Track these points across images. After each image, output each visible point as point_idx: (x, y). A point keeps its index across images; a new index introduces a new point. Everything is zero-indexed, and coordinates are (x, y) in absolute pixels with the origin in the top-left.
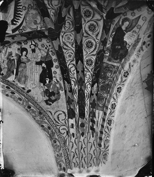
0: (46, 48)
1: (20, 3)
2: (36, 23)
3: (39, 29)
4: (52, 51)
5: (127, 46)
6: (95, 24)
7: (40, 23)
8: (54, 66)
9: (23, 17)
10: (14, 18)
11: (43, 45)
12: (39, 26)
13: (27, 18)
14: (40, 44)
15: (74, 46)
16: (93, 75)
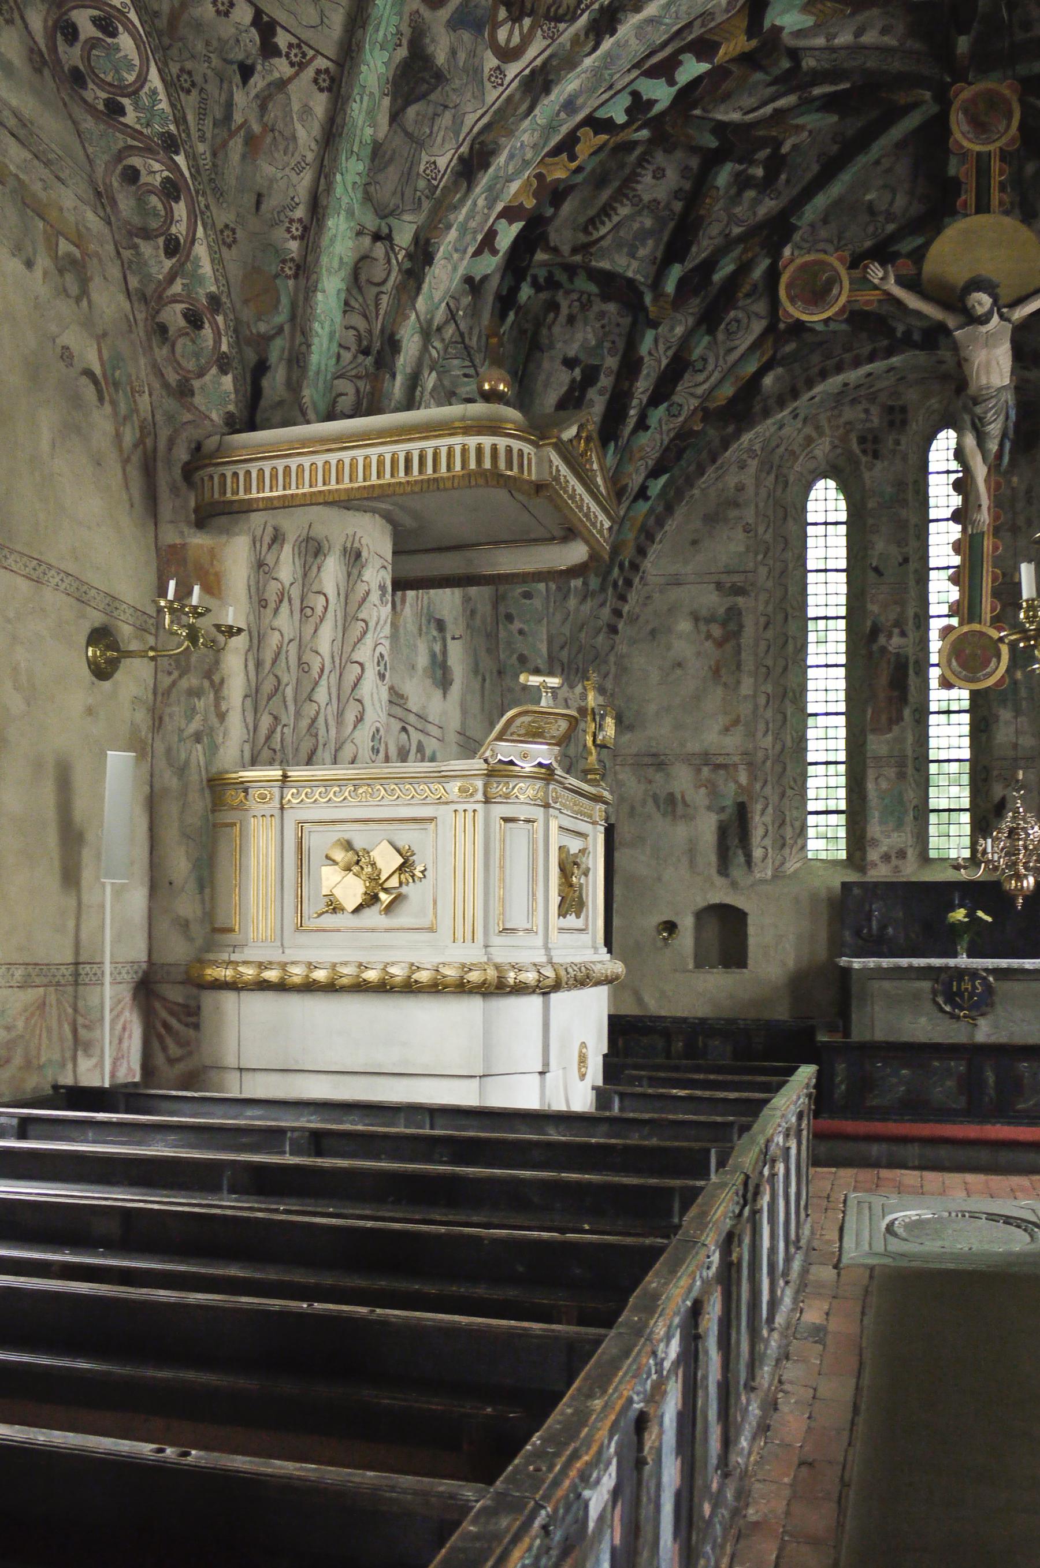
0: (603, 327)
1: (638, 182)
2: (632, 255)
3: (630, 274)
4: (613, 342)
5: (759, 398)
6: (745, 321)
7: (642, 260)
8: (599, 384)
9: (616, 219)
10: (598, 215)
11: (602, 315)
12: (635, 264)
13: (622, 233)
14: (598, 306)
15: (670, 353)
16: (667, 449)
